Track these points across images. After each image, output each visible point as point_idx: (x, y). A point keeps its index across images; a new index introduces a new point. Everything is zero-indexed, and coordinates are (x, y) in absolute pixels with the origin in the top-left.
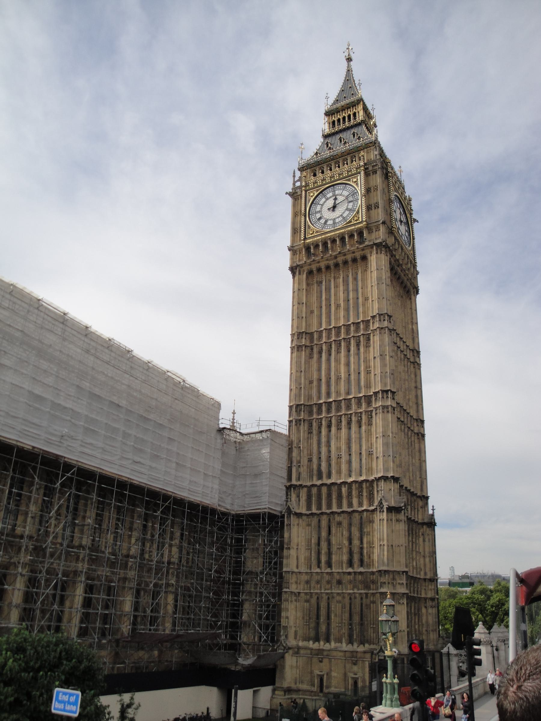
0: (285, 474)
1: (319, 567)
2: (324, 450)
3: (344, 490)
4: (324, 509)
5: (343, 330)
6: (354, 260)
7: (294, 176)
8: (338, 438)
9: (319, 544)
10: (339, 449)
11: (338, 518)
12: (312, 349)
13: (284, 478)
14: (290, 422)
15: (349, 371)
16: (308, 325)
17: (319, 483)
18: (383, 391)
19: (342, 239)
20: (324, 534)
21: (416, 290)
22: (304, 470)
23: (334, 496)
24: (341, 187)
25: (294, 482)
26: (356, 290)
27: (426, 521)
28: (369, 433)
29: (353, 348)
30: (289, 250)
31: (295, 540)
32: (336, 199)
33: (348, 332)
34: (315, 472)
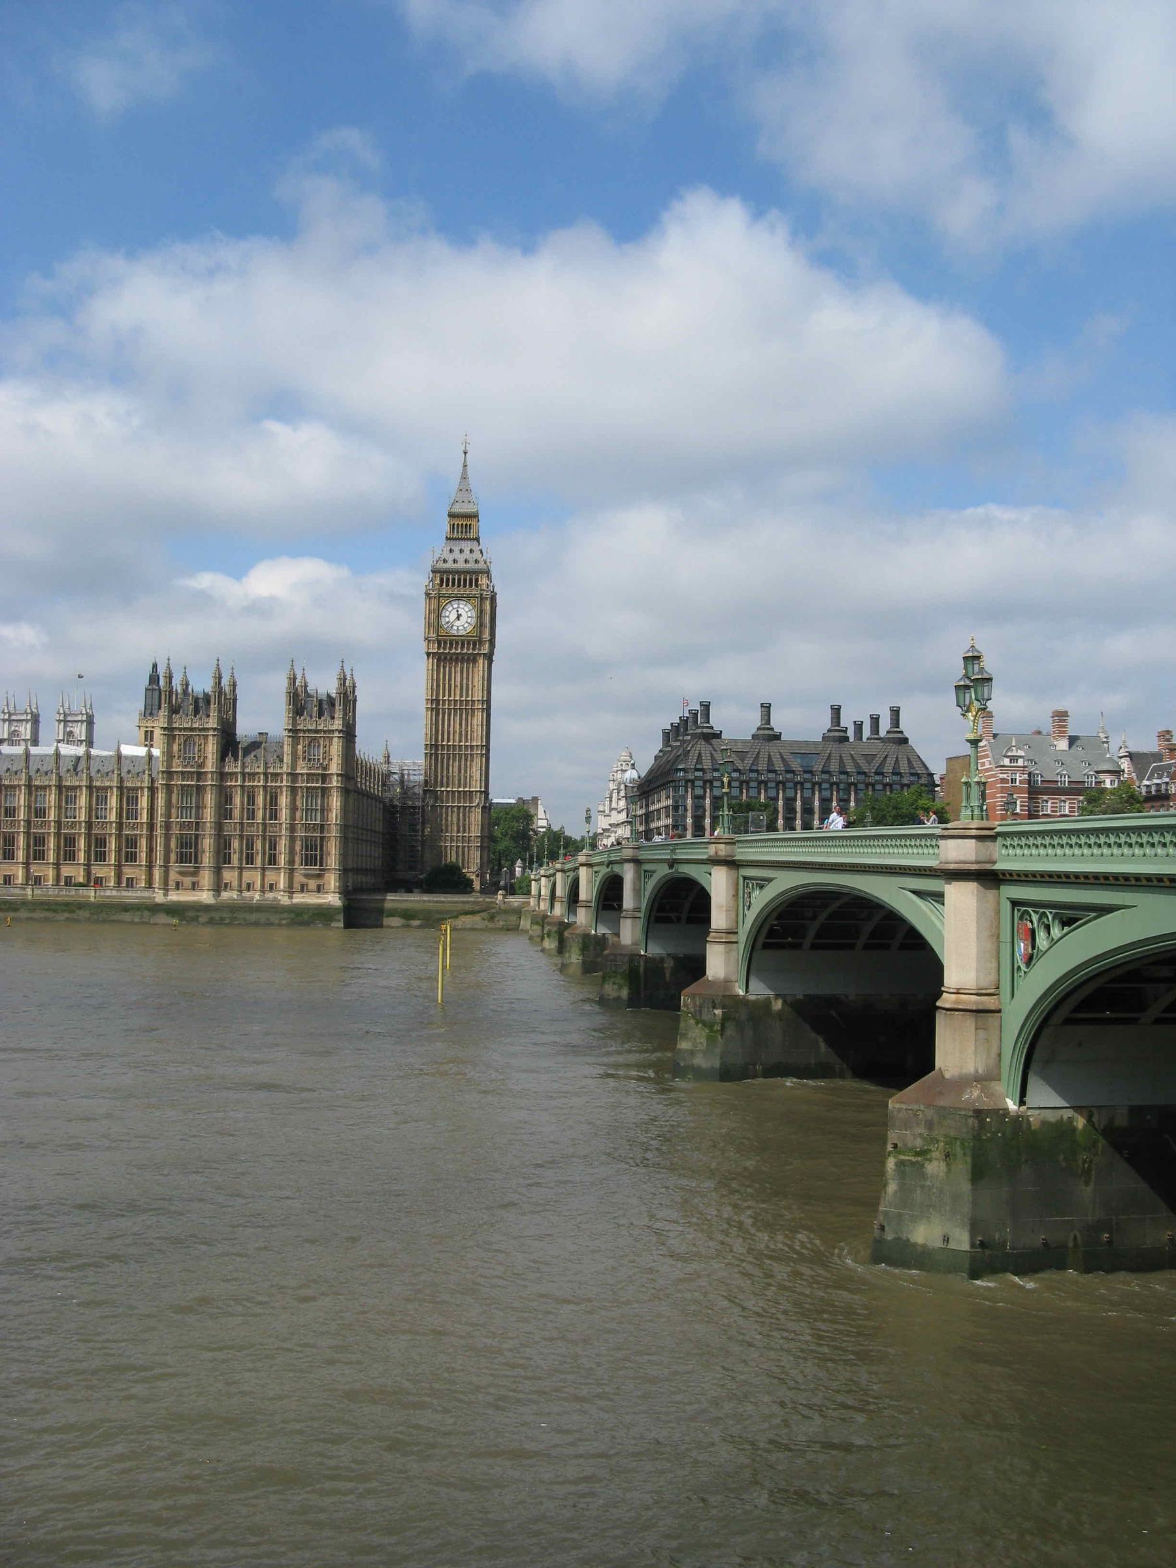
2: (445, 772)
19: (463, 645)
24: (464, 603)
26: (468, 679)
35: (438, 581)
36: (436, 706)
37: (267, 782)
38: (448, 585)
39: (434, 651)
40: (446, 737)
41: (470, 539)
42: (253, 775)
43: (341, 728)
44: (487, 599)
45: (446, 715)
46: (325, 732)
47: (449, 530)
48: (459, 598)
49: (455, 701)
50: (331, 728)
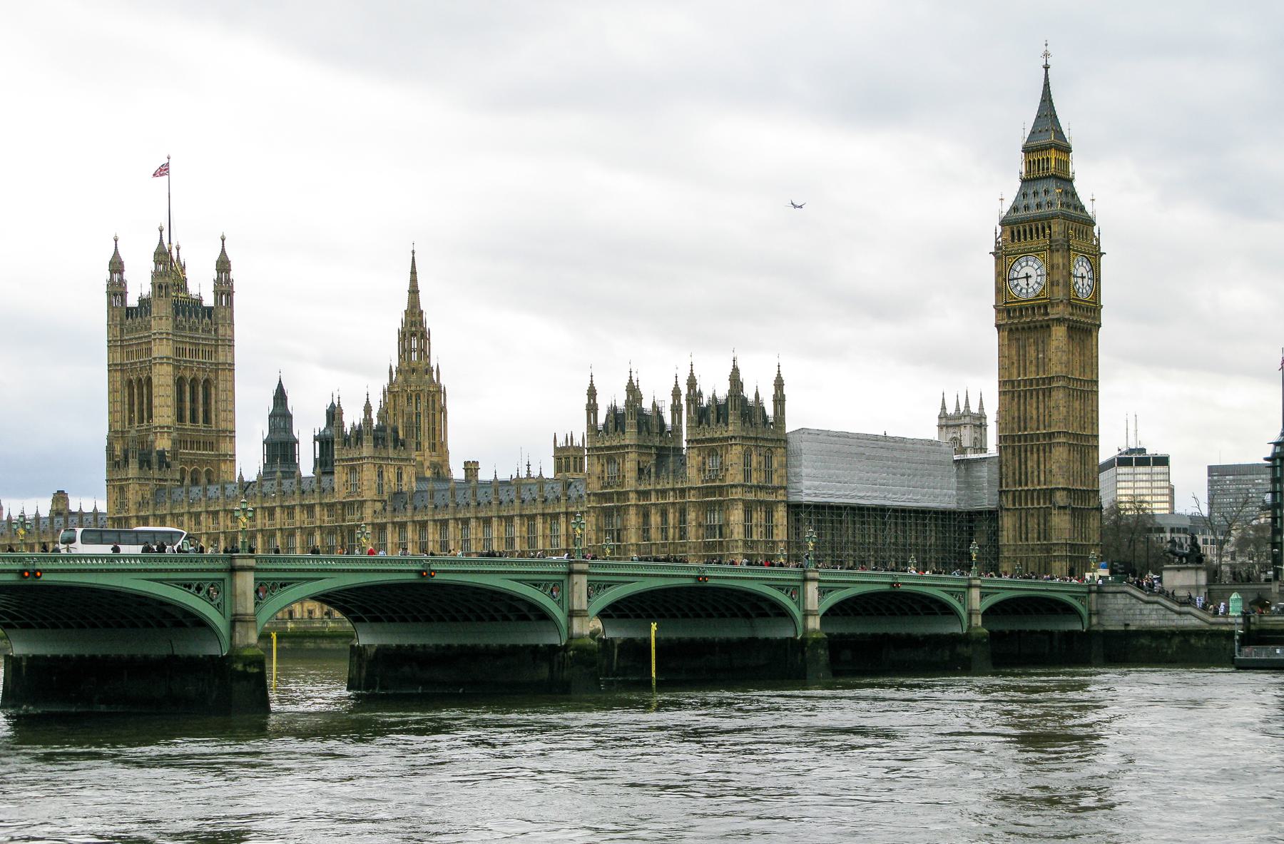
0: (998, 484)
1: (1021, 540)
2: (1023, 467)
3: (1035, 494)
4: (1023, 506)
6: (1042, 327)
8: (1032, 460)
10: (1032, 467)
11: (1031, 511)
12: (1013, 392)
15: (1038, 412)
17: (1020, 489)
18: (1058, 432)
19: (1033, 309)
20: (1023, 521)
21: (1099, 326)
22: (1010, 480)
25: (1004, 488)
28: (1050, 459)
29: (1041, 397)
31: (1006, 526)
38: (1019, 240)
40: (1022, 424)
42: (663, 493)
43: (731, 434)
44: (1058, 251)
45: (1022, 401)
46: (720, 440)
48: (1026, 253)
49: (1032, 380)
50: (725, 435)
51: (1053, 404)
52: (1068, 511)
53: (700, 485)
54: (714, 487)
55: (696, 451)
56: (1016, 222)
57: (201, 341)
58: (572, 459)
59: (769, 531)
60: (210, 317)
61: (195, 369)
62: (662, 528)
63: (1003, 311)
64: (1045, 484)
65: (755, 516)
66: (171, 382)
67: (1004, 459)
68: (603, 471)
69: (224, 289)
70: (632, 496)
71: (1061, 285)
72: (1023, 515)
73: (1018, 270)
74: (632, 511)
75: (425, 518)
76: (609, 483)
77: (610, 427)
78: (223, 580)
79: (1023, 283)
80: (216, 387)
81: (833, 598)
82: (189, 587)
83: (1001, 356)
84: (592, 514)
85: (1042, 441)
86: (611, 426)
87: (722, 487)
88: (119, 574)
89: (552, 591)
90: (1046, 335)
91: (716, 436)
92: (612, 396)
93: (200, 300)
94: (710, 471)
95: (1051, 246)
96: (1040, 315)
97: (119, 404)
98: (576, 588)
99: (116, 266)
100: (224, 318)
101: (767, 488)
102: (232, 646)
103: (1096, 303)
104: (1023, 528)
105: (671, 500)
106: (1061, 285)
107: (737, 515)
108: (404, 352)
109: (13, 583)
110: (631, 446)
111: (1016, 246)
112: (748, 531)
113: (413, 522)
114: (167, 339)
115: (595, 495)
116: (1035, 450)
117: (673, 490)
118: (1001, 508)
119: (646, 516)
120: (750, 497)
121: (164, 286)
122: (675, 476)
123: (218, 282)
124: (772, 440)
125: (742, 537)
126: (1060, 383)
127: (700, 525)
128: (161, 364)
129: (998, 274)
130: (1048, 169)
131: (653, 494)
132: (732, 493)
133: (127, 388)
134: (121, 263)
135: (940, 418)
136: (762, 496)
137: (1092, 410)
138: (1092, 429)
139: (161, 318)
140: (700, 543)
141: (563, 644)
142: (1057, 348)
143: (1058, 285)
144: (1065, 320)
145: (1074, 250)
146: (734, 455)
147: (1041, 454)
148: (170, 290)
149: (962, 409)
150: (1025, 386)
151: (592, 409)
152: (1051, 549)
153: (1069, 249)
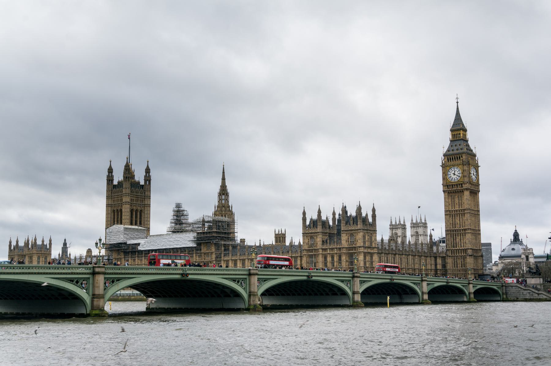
2: (455, 241)
3: (460, 251)
5: (458, 211)
7: (442, 159)
8: (458, 239)
9: (454, 263)
11: (459, 257)
12: (450, 215)
13: (442, 236)
14: (446, 234)
15: (460, 221)
16: (449, 208)
17: (454, 249)
19: (457, 185)
21: (479, 191)
23: (457, 252)
24: (456, 168)
25: (448, 249)
26: (461, 200)
27: (481, 255)
28: (465, 238)
29: (461, 216)
30: (442, 184)
32: (455, 171)
33: (459, 212)
34: (453, 246)
35: (446, 160)
36: (449, 213)
37: (337, 251)
39: (446, 190)
40: (454, 226)
41: (459, 140)
42: (332, 249)
43: (359, 228)
44: (465, 165)
45: (454, 218)
46: (355, 230)
47: (451, 138)
48: (454, 166)
50: (357, 228)
51: (465, 218)
52: (473, 257)
53: (347, 246)
54: (353, 247)
55: (345, 234)
56: (449, 155)
57: (139, 197)
58: (281, 238)
59: (372, 263)
60: (143, 189)
61: (137, 206)
62: (332, 262)
63: (446, 186)
64: (463, 247)
65: (367, 258)
66: (129, 210)
67: (447, 238)
68: (309, 242)
69: (148, 179)
70: (321, 250)
71: (467, 177)
72: (455, 258)
73: (451, 172)
74: (320, 256)
75: (236, 258)
76: (311, 246)
77: (311, 226)
78: (246, 278)
79: (452, 175)
80: (144, 213)
81: (431, 287)
82: (235, 281)
83: (445, 202)
84: (305, 257)
85: (461, 231)
86: (312, 225)
87: (356, 247)
88: (214, 276)
89: (347, 284)
90: (462, 194)
91: (353, 229)
92: (312, 215)
93: (139, 183)
94: (351, 242)
95: (463, 163)
96: (460, 187)
97: (110, 218)
98: (356, 283)
99: (110, 170)
100: (147, 189)
101: (370, 248)
102: (249, 305)
103: (478, 183)
104: (456, 263)
105: (336, 252)
106: (467, 177)
107: (361, 257)
108: (220, 200)
109: (179, 279)
110: (320, 232)
111: (450, 163)
112: (365, 263)
113: (232, 260)
114: (128, 196)
115: (306, 250)
116: (459, 235)
117: (336, 248)
118: (447, 256)
119: (325, 258)
120: (366, 251)
121: (128, 177)
122: (337, 244)
123: (145, 176)
124: (372, 230)
125: (363, 265)
126: (468, 211)
127: (347, 261)
128: (126, 204)
129: (443, 173)
130: (460, 137)
131: (328, 250)
132: (360, 249)
133: (112, 213)
134: (112, 169)
135: (390, 225)
136: (369, 251)
137: (478, 221)
138: (478, 228)
139: (126, 189)
140: (347, 268)
141: (351, 304)
142: (466, 199)
143: (466, 177)
144: (470, 189)
145: (471, 165)
146: (360, 235)
147: (462, 236)
148: (130, 179)
149: (398, 223)
150: (455, 212)
151: (304, 219)
152: (467, 271)
153: (469, 165)
